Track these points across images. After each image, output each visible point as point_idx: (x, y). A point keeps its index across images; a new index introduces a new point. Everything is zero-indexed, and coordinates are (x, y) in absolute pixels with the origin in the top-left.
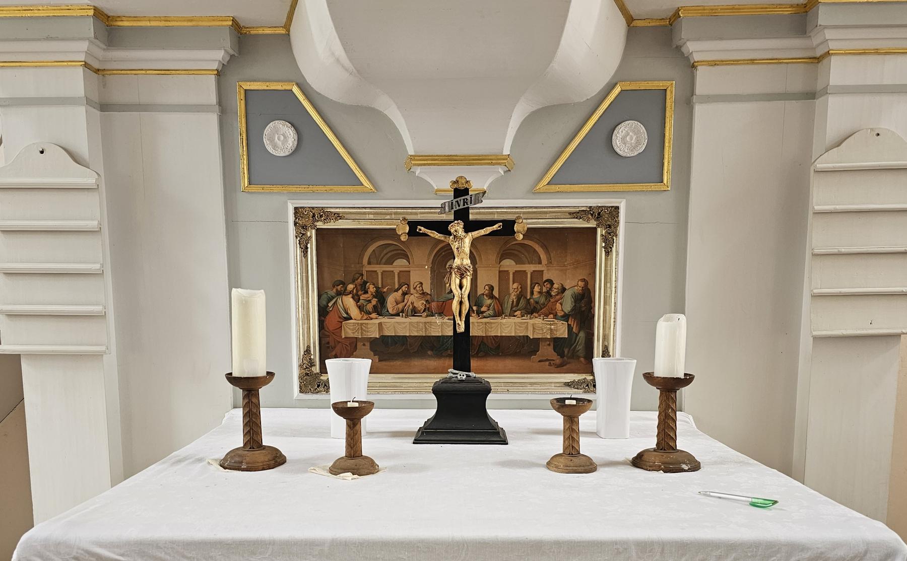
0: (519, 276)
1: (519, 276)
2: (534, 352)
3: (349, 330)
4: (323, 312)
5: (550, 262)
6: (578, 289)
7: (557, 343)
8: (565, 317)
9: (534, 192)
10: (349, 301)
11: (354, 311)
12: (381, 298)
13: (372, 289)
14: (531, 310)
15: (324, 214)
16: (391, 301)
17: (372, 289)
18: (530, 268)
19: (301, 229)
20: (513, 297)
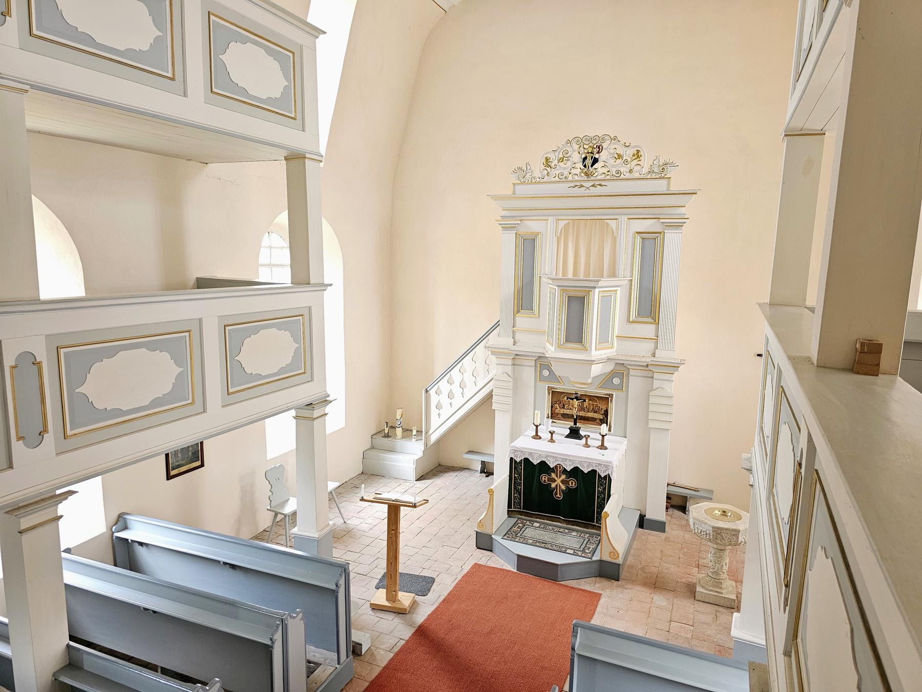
0: (593, 405)
1: (593, 405)
2: (596, 421)
3: (557, 411)
4: (552, 407)
5: (599, 403)
6: (605, 409)
7: (600, 420)
8: (602, 414)
9: (596, 389)
10: (557, 405)
11: (558, 407)
12: (564, 406)
13: (562, 403)
14: (595, 412)
15: (553, 388)
16: (566, 406)
17: (562, 403)
18: (595, 404)
19: (549, 390)
20: (591, 409)
